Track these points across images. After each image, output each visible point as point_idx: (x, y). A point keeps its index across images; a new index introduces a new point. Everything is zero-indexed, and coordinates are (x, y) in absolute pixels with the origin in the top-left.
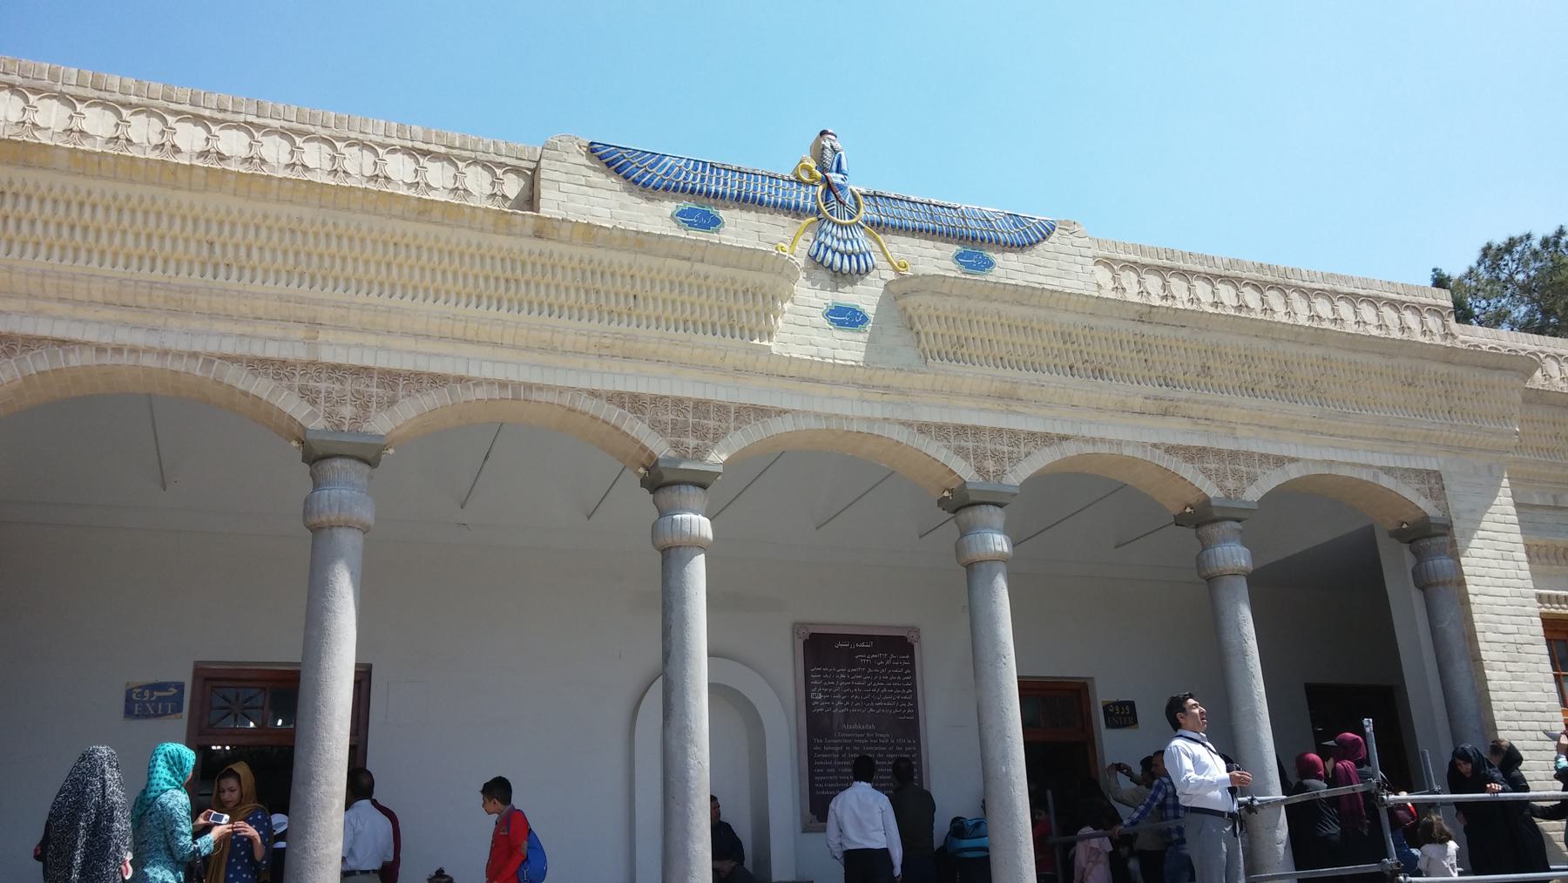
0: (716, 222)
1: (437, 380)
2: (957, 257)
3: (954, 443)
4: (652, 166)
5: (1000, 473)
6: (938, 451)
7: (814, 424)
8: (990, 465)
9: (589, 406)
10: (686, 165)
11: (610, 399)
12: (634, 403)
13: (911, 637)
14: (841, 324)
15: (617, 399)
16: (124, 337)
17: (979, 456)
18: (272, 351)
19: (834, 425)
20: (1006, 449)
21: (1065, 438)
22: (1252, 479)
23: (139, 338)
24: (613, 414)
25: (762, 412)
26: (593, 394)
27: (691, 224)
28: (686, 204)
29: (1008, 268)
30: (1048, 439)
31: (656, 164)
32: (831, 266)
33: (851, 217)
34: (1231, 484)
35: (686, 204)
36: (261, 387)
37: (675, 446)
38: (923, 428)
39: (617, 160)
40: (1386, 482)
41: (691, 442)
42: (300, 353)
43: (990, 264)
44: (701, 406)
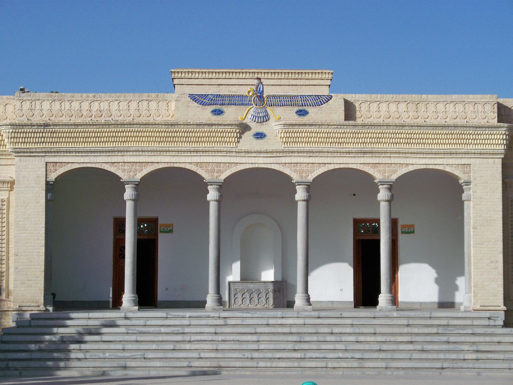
0: (222, 112)
2: (296, 113)
9: (188, 167)
14: (257, 138)
17: (301, 172)
22: (395, 172)
27: (215, 114)
28: (214, 107)
29: (315, 114)
34: (386, 174)
35: (214, 107)
40: (448, 169)
41: (216, 174)
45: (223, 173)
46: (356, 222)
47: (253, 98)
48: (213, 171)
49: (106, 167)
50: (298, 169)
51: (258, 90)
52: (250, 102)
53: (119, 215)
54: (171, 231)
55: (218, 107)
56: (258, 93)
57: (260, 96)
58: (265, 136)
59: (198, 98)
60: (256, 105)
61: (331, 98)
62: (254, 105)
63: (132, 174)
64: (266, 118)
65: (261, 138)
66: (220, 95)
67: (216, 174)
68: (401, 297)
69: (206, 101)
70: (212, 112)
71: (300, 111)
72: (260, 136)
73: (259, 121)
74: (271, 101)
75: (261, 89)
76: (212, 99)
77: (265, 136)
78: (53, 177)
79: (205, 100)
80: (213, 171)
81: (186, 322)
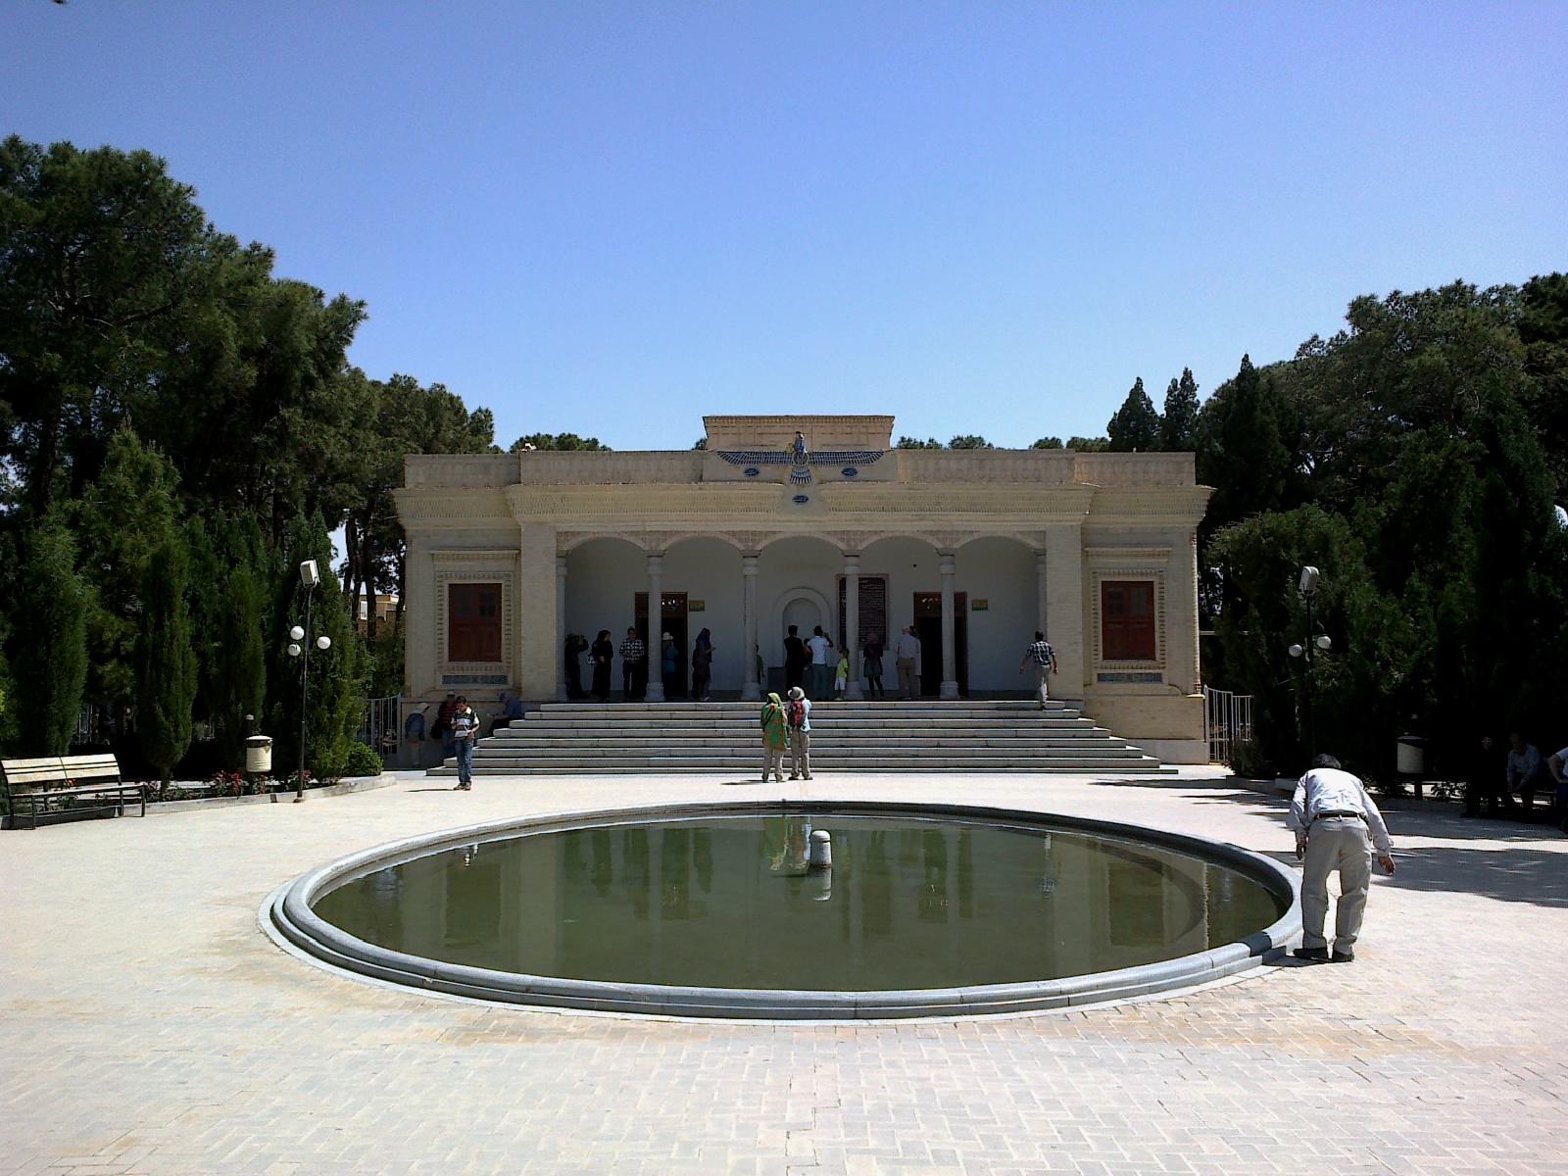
1: (677, 532)
5: (856, 545)
6: (833, 540)
8: (853, 543)
9: (719, 536)
12: (733, 534)
13: (884, 578)
15: (728, 533)
16: (598, 529)
18: (634, 529)
21: (882, 531)
22: (958, 540)
23: (603, 529)
24: (726, 537)
25: (774, 533)
30: (876, 533)
34: (948, 543)
36: (632, 539)
38: (829, 533)
40: (1019, 537)
41: (750, 544)
42: (640, 529)
43: (856, 473)
44: (754, 533)
45: (758, 543)
46: (916, 596)
48: (746, 540)
49: (626, 537)
53: (642, 590)
54: (703, 609)
55: (753, 466)
63: (654, 544)
64: (807, 479)
67: (750, 544)
68: (972, 685)
72: (801, 499)
77: (807, 499)
78: (565, 548)
80: (746, 540)
81: (718, 714)
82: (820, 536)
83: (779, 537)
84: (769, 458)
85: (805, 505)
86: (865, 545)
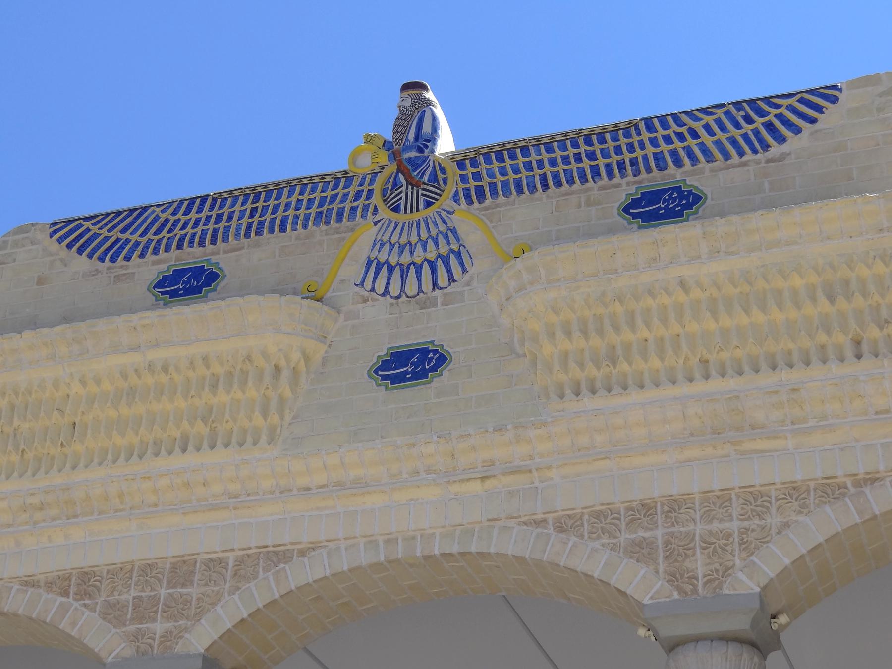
2: (626, 210)
3: (625, 537)
4: (123, 231)
6: (592, 559)
7: (364, 559)
8: (699, 564)
10: (174, 213)
11: (49, 585)
12: (81, 585)
14: (397, 379)
15: (60, 584)
19: (400, 552)
20: (734, 526)
24: (47, 606)
25: (278, 556)
26: (29, 583)
31: (132, 223)
32: (386, 293)
33: (428, 204)
37: (136, 637)
39: (81, 236)
47: (380, 179)
48: (144, 610)
50: (659, 534)
51: (411, 136)
52: (361, 202)
55: (192, 256)
56: (407, 148)
57: (415, 163)
58: (442, 359)
59: (95, 229)
60: (396, 209)
61: (834, 100)
62: (385, 213)
65: (420, 375)
66: (204, 199)
67: (159, 627)
69: (134, 238)
70: (159, 285)
71: (651, 197)
72: (410, 365)
73: (411, 289)
74: (477, 177)
75: (427, 128)
76: (167, 221)
77: (442, 359)
79: (127, 235)
80: (144, 610)
82: (514, 543)
83: (299, 574)
84: (262, 208)
85: (443, 379)
86: (774, 560)
